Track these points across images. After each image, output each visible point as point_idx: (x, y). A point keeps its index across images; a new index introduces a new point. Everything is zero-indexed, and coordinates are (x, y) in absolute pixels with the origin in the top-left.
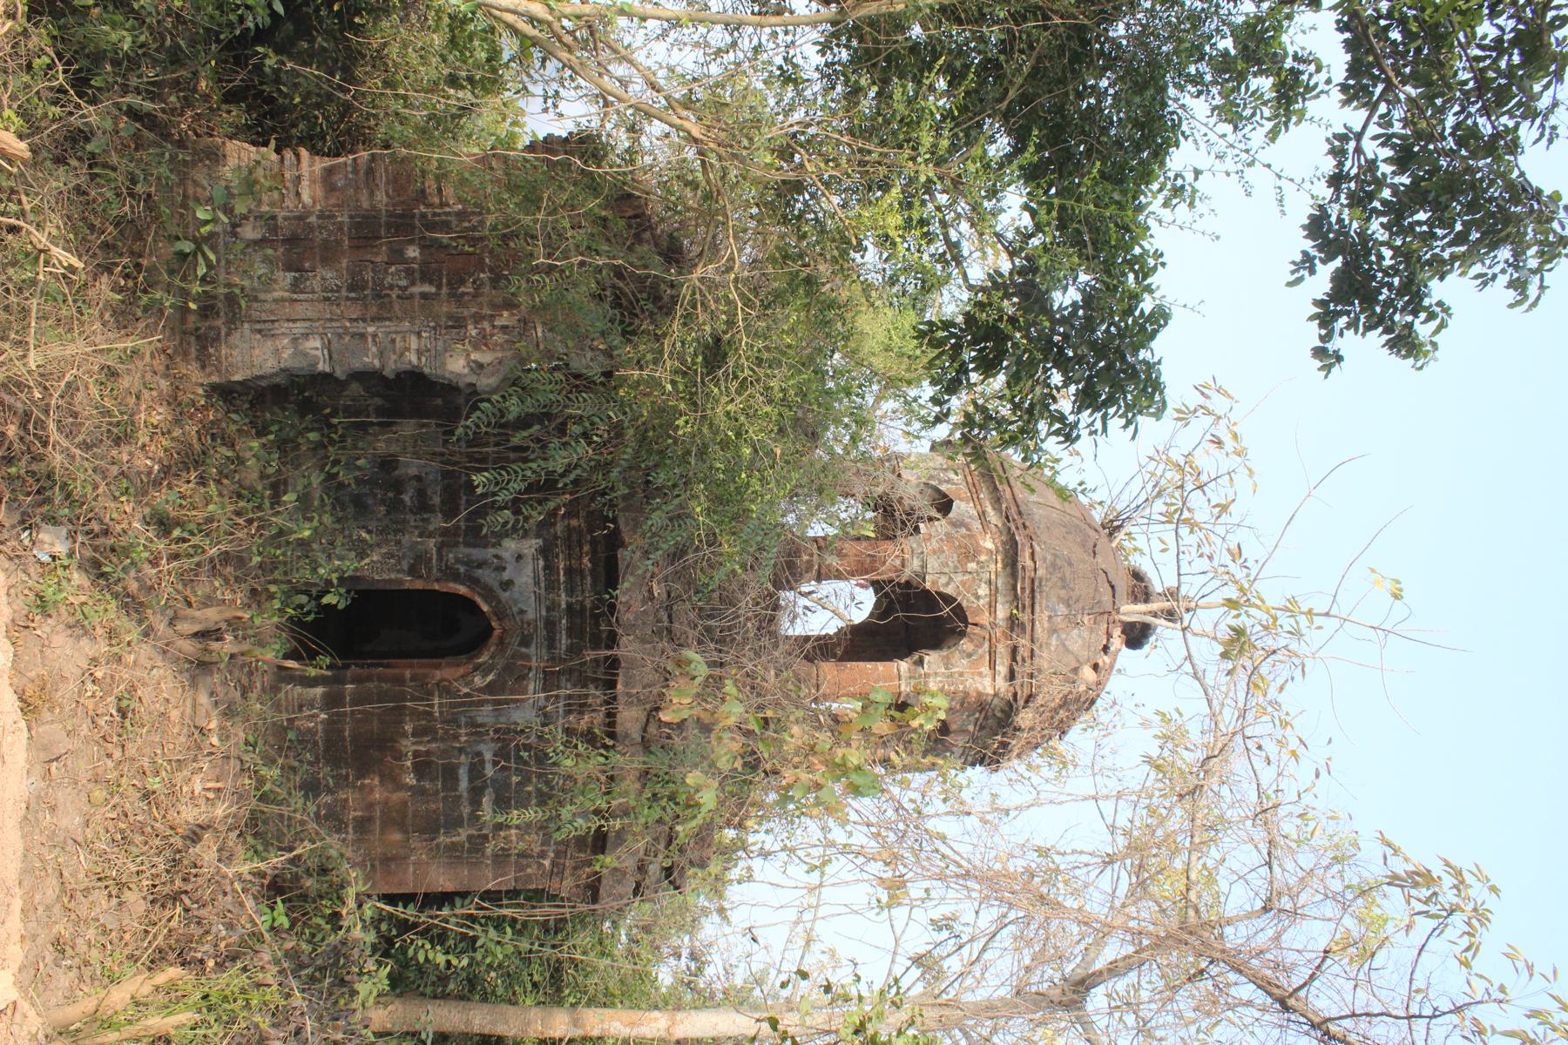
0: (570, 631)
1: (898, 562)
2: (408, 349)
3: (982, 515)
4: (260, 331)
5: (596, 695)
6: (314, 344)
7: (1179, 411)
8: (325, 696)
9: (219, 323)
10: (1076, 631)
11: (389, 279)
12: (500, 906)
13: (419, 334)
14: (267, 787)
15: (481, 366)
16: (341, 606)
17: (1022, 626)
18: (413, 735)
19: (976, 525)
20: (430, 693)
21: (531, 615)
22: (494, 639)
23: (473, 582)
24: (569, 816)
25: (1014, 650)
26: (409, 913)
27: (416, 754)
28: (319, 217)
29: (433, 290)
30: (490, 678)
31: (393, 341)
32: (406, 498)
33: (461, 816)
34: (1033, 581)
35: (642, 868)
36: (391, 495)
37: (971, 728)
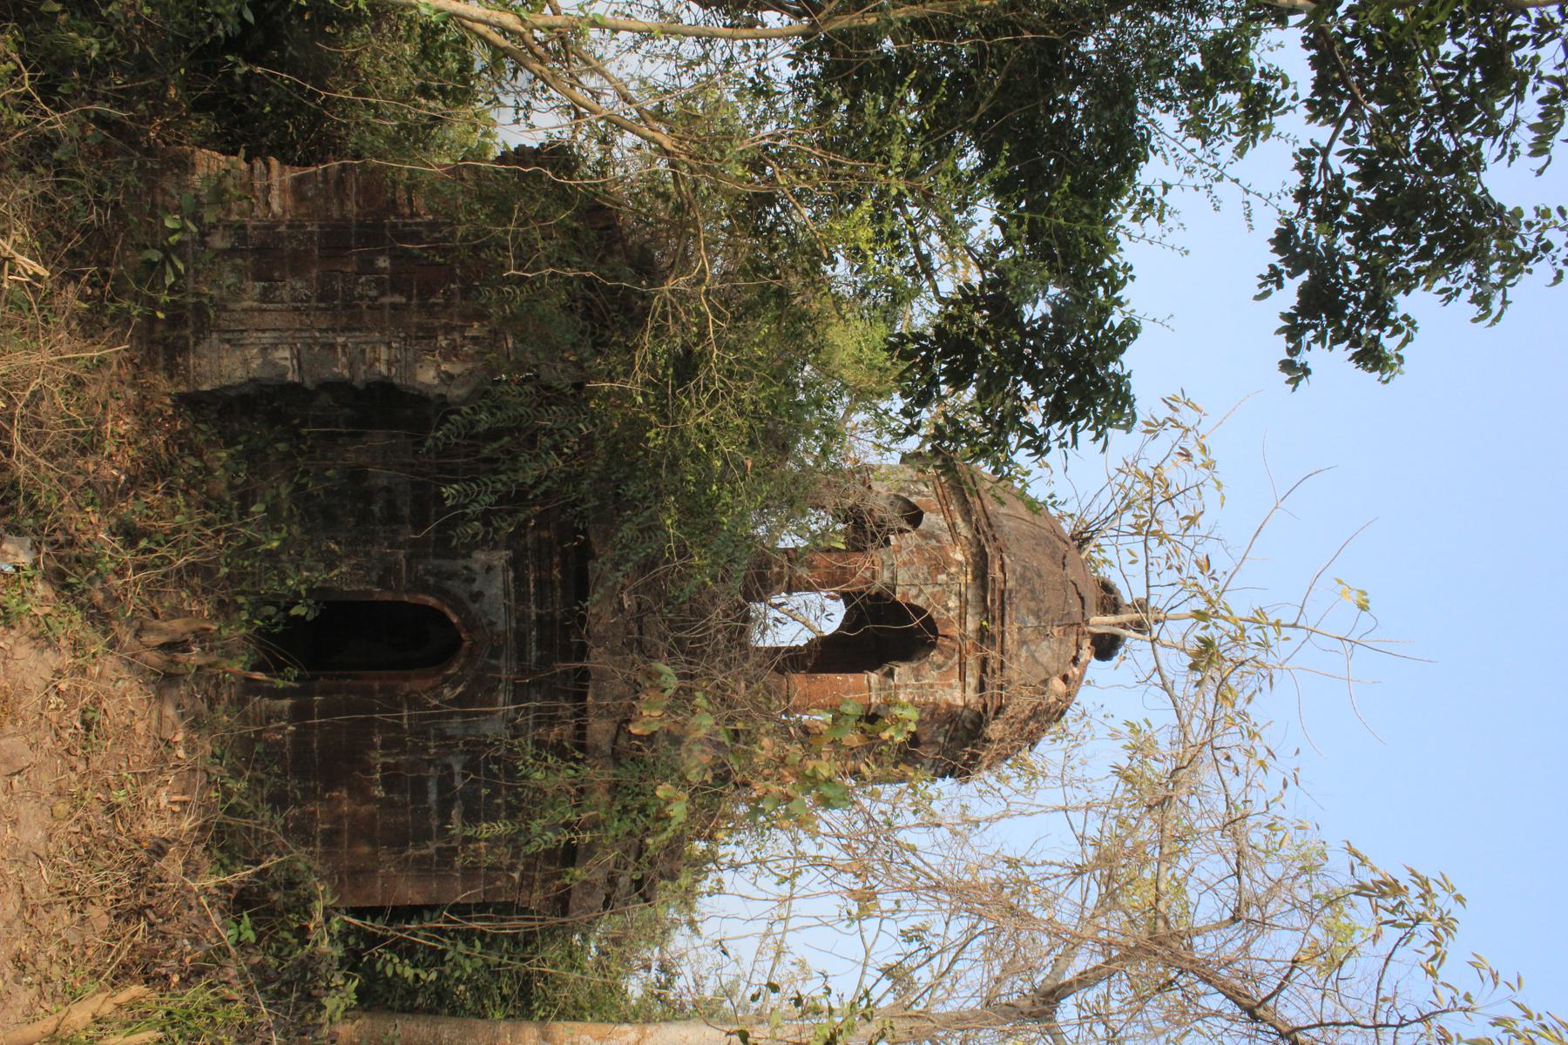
0: (540, 644)
1: (868, 574)
2: (378, 360)
3: (952, 527)
4: (228, 341)
5: (566, 707)
6: (283, 355)
7: (1147, 424)
8: (293, 708)
9: (188, 332)
10: (1045, 643)
11: (359, 289)
12: (470, 920)
13: (389, 345)
14: (233, 800)
15: (451, 377)
16: (309, 618)
17: (992, 638)
18: (382, 747)
19: (947, 537)
20: (398, 706)
21: (500, 627)
22: (463, 652)
23: (443, 593)
24: (539, 830)
25: (984, 663)
26: (376, 926)
27: (385, 767)
28: (289, 227)
29: (404, 300)
30: (460, 689)
31: (363, 352)
32: (376, 508)
33: (430, 828)
34: (1002, 593)
35: (612, 881)
36: (360, 505)
37: (941, 739)
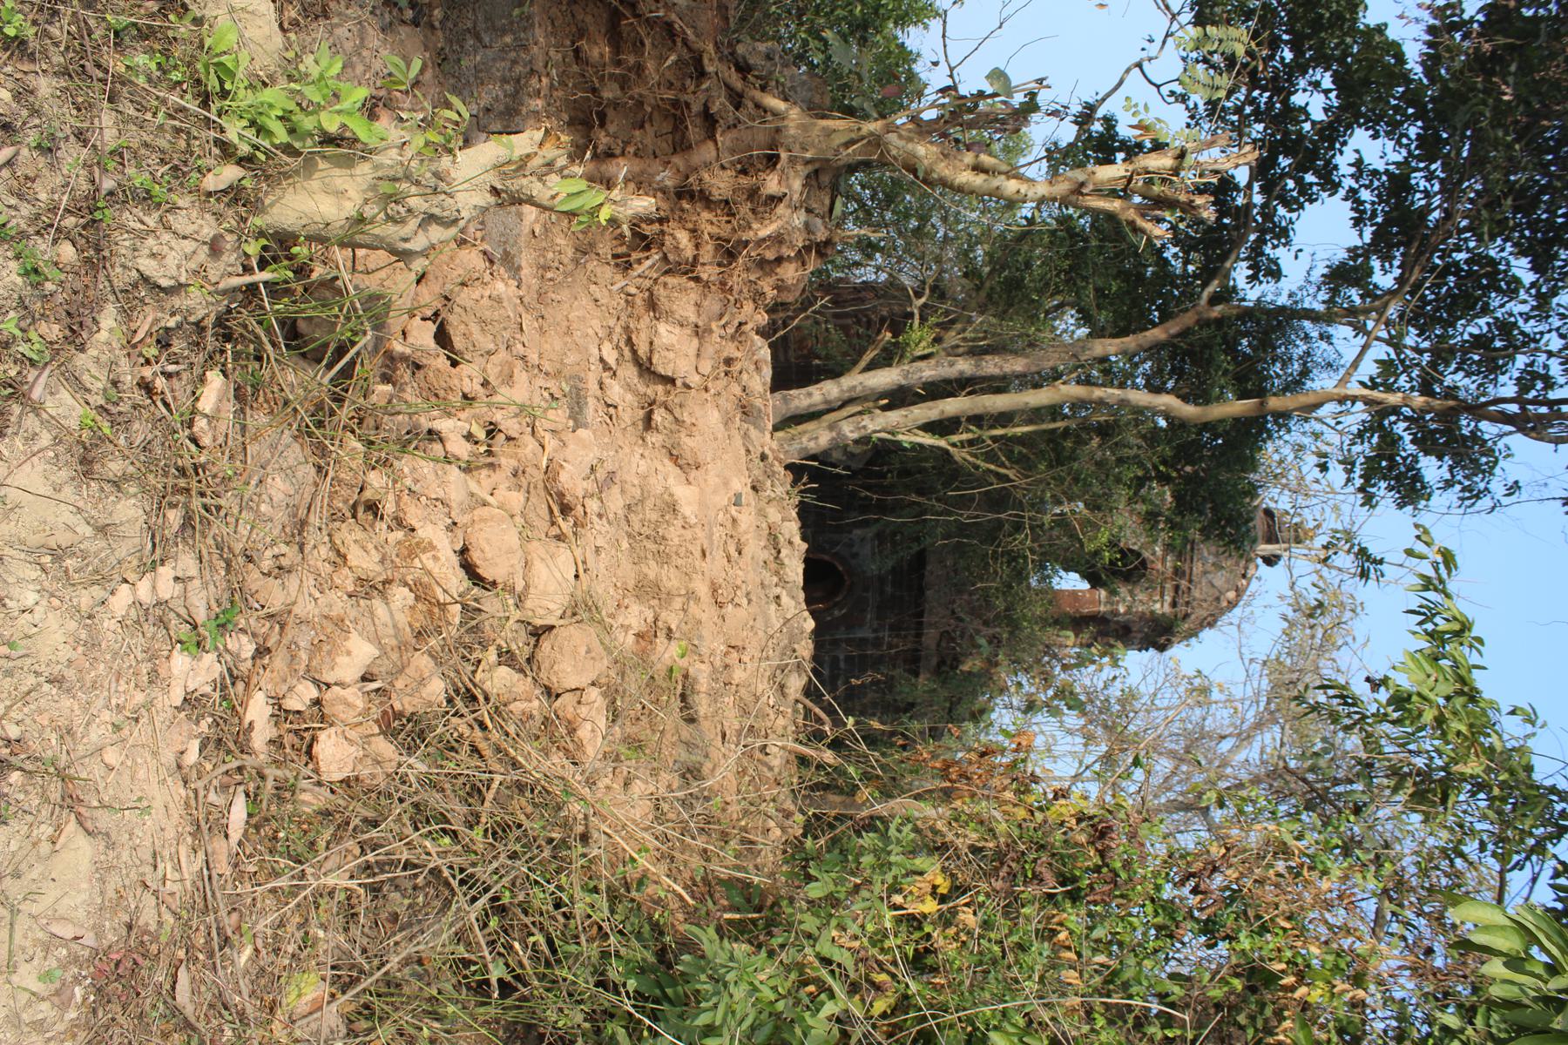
17: (1184, 573)
25: (1177, 588)
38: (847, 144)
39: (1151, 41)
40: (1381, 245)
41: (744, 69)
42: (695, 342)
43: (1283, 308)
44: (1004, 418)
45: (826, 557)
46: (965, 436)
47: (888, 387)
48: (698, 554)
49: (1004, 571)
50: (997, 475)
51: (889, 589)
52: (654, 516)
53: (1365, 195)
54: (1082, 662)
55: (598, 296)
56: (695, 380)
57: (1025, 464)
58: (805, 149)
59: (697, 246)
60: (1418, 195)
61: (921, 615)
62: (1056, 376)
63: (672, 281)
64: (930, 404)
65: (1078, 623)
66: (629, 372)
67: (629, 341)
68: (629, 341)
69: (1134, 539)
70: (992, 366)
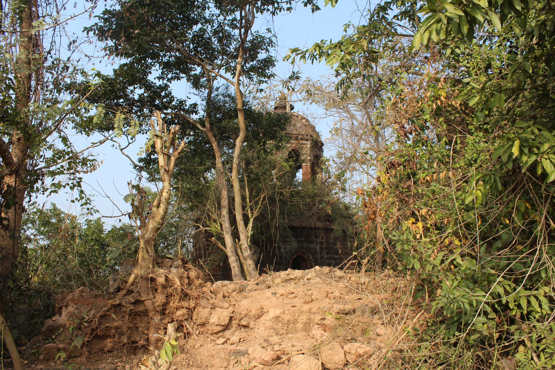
25: (302, 139)
38: (148, 252)
39: (113, 146)
40: (186, 71)
41: (119, 289)
42: (217, 309)
43: (207, 103)
44: (243, 198)
45: (291, 261)
46: (249, 212)
47: (232, 239)
48: (294, 308)
49: (297, 198)
50: (263, 201)
51: (302, 239)
52: (280, 325)
53: (170, 76)
54: (328, 172)
55: (199, 345)
56: (231, 309)
57: (259, 191)
58: (149, 268)
59: (183, 308)
60: (171, 59)
61: (311, 228)
62: (229, 180)
63: (195, 317)
64: (238, 224)
65: (314, 172)
66: (227, 333)
67: (216, 333)
68: (216, 333)
69: (285, 154)
70: (225, 202)
